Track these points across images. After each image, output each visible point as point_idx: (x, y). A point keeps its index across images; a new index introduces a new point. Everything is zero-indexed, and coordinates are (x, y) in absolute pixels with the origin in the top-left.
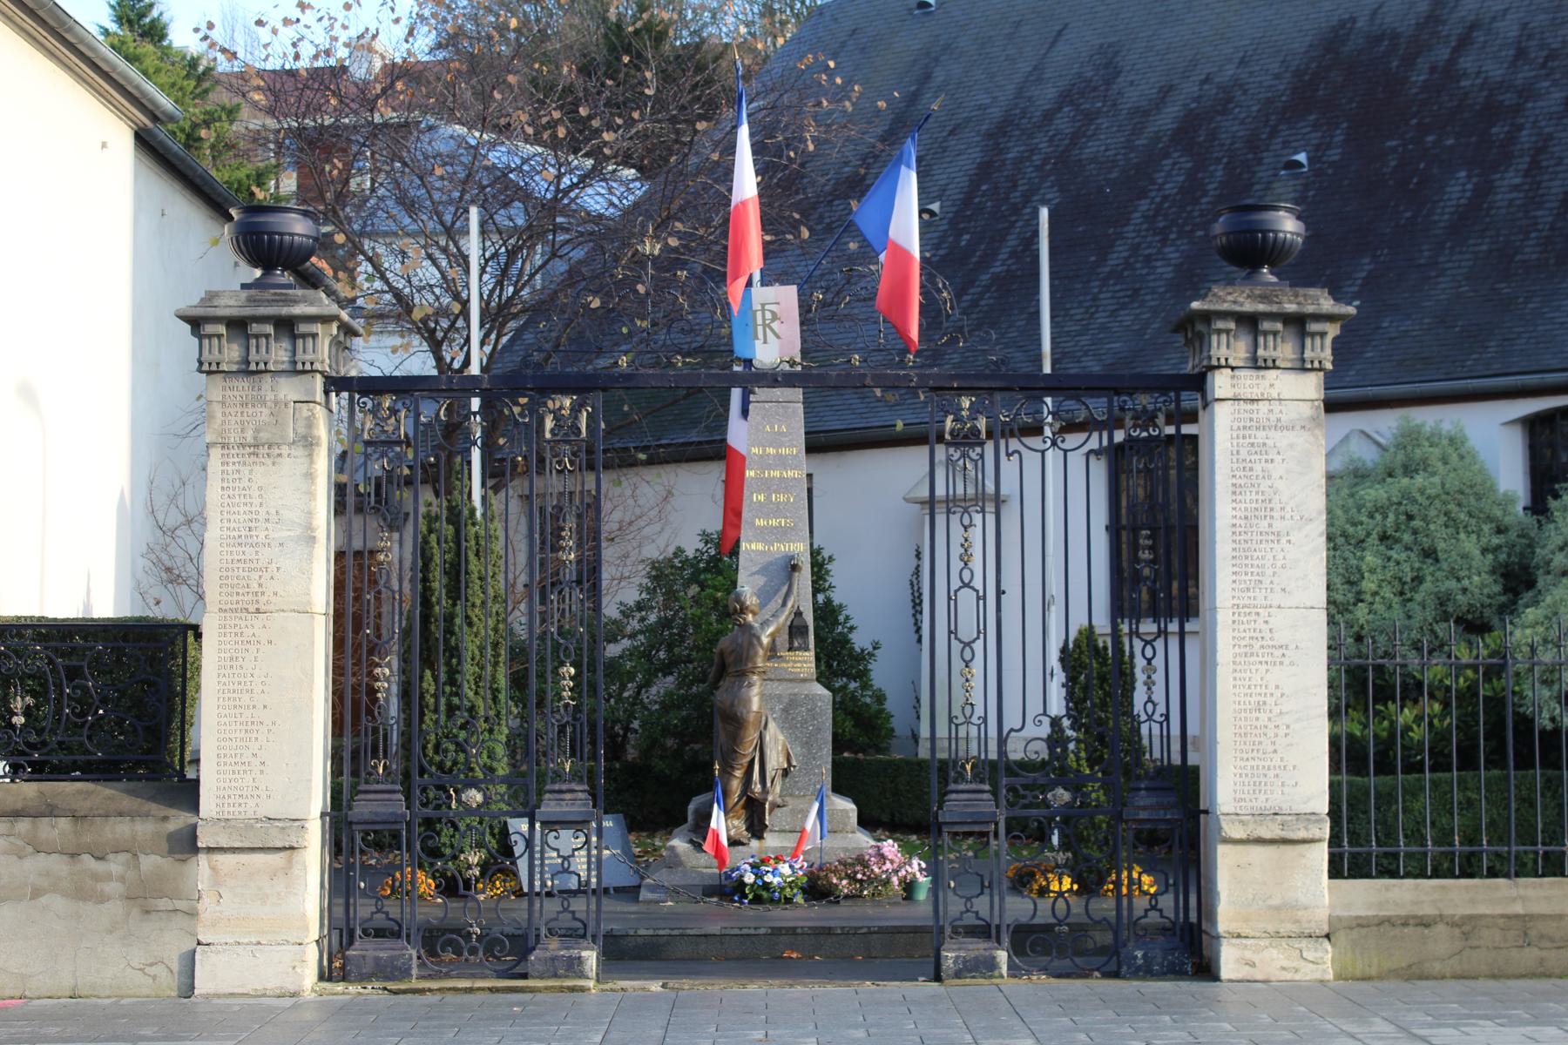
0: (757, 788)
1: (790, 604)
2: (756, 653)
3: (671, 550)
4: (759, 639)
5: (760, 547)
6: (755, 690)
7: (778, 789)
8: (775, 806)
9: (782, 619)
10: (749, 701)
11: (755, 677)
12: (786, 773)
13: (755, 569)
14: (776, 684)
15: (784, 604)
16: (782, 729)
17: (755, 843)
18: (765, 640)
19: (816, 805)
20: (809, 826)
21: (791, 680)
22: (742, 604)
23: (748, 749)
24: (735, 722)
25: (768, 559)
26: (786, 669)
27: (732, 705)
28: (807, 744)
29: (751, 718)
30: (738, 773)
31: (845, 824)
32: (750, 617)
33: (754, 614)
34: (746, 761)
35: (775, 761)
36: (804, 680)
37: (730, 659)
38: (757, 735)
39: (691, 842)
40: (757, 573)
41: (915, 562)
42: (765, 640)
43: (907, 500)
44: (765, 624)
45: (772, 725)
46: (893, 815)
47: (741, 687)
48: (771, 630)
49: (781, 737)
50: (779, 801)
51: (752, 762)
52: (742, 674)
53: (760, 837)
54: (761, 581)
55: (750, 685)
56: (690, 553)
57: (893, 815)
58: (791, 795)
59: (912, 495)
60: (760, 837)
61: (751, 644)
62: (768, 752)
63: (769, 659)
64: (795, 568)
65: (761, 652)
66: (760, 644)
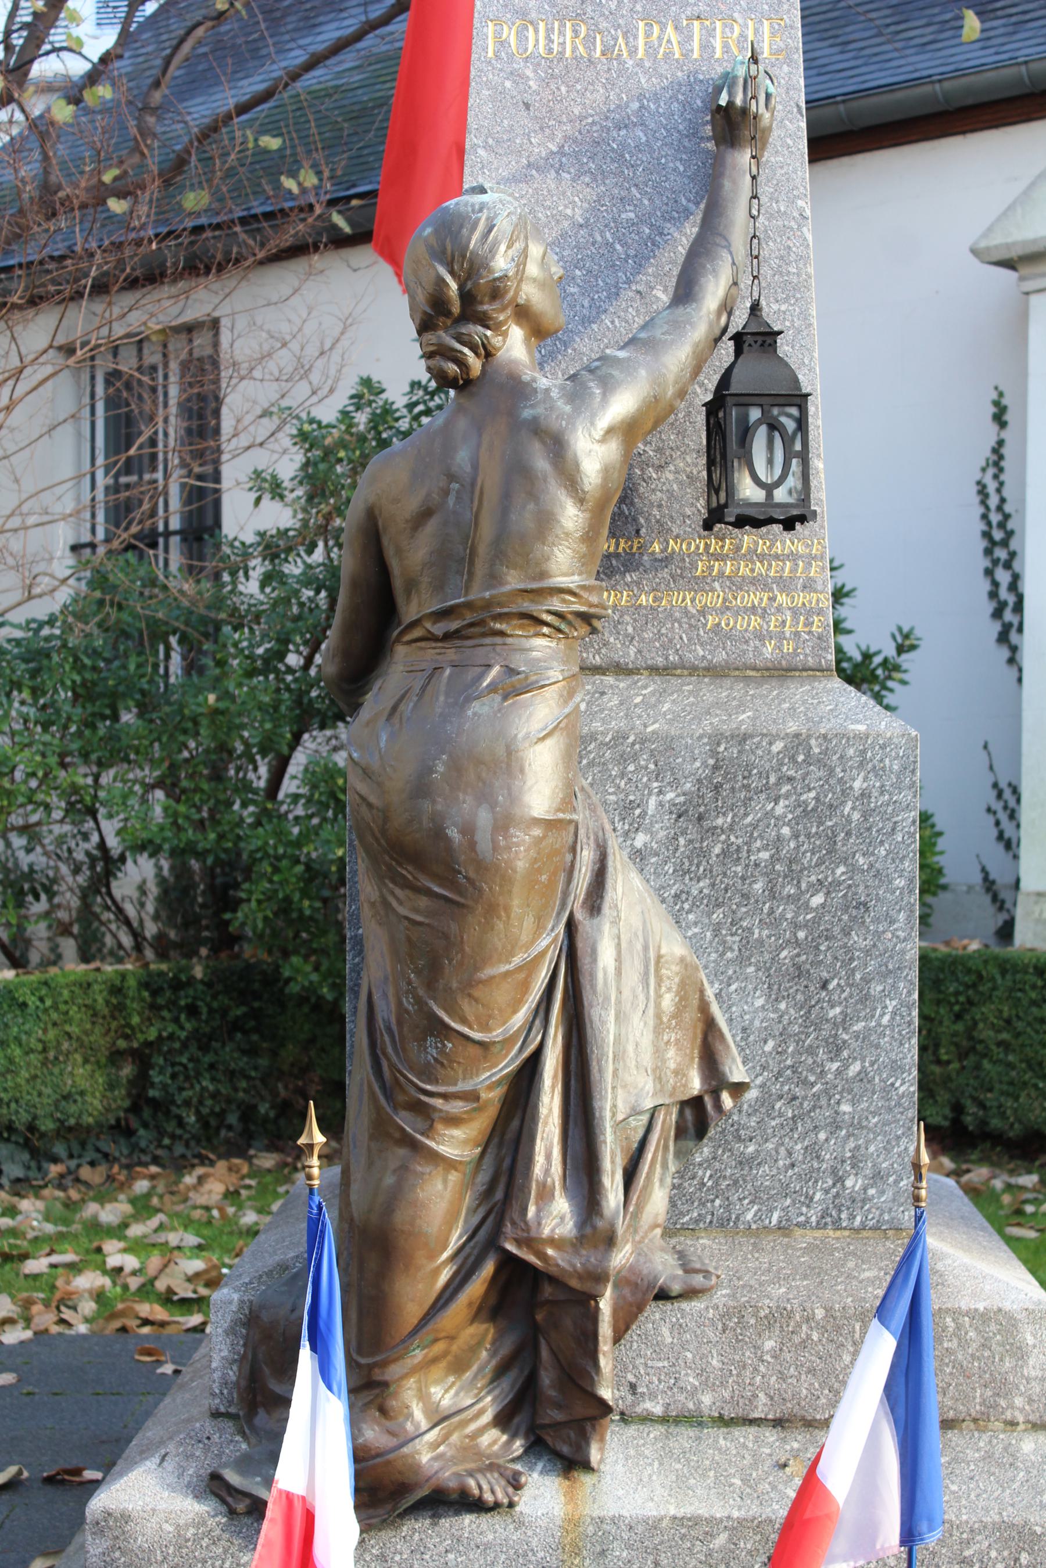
0: (555, 1216)
1: (713, 292)
2: (546, 521)
3: (348, 386)
4: (557, 447)
5: (568, 41)
6: (541, 711)
7: (657, 1201)
8: (650, 1294)
9: (678, 357)
10: (507, 764)
11: (541, 646)
12: (695, 1119)
13: (541, 146)
14: (649, 686)
15: (686, 291)
16: (677, 905)
17: (543, 1495)
18: (593, 454)
19: (881, 1348)
20: (838, 1478)
21: (715, 672)
22: (470, 269)
23: (507, 1019)
24: (438, 873)
25: (595, 98)
26: (693, 620)
27: (421, 788)
28: (800, 979)
29: (521, 852)
30: (456, 1143)
31: (1002, 1387)
32: (514, 345)
33: (538, 331)
34: (490, 1079)
35: (639, 1070)
36: (781, 672)
37: (412, 555)
38: (549, 941)
39: (215, 1486)
40: (555, 163)
41: (990, 433)
42: (593, 454)
43: (974, 252)
44: (591, 379)
45: (628, 889)
46: (958, 1109)
47: (465, 694)
48: (623, 404)
49: (674, 947)
50: (664, 1267)
51: (532, 1065)
52: (473, 626)
53: (572, 1463)
54: (571, 201)
55: (516, 686)
56: (397, 395)
57: (958, 1109)
58: (724, 1224)
59: (997, 239)
60: (572, 1463)
61: (519, 477)
62: (606, 1025)
63: (611, 568)
64: (731, 125)
65: (571, 516)
66: (569, 475)
